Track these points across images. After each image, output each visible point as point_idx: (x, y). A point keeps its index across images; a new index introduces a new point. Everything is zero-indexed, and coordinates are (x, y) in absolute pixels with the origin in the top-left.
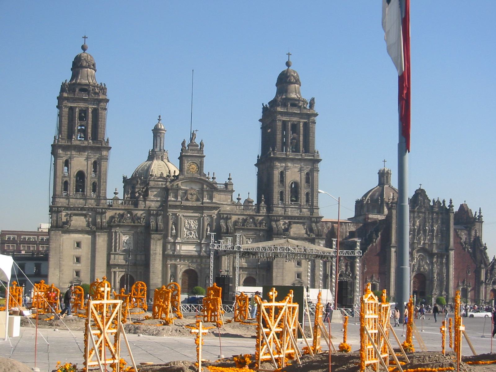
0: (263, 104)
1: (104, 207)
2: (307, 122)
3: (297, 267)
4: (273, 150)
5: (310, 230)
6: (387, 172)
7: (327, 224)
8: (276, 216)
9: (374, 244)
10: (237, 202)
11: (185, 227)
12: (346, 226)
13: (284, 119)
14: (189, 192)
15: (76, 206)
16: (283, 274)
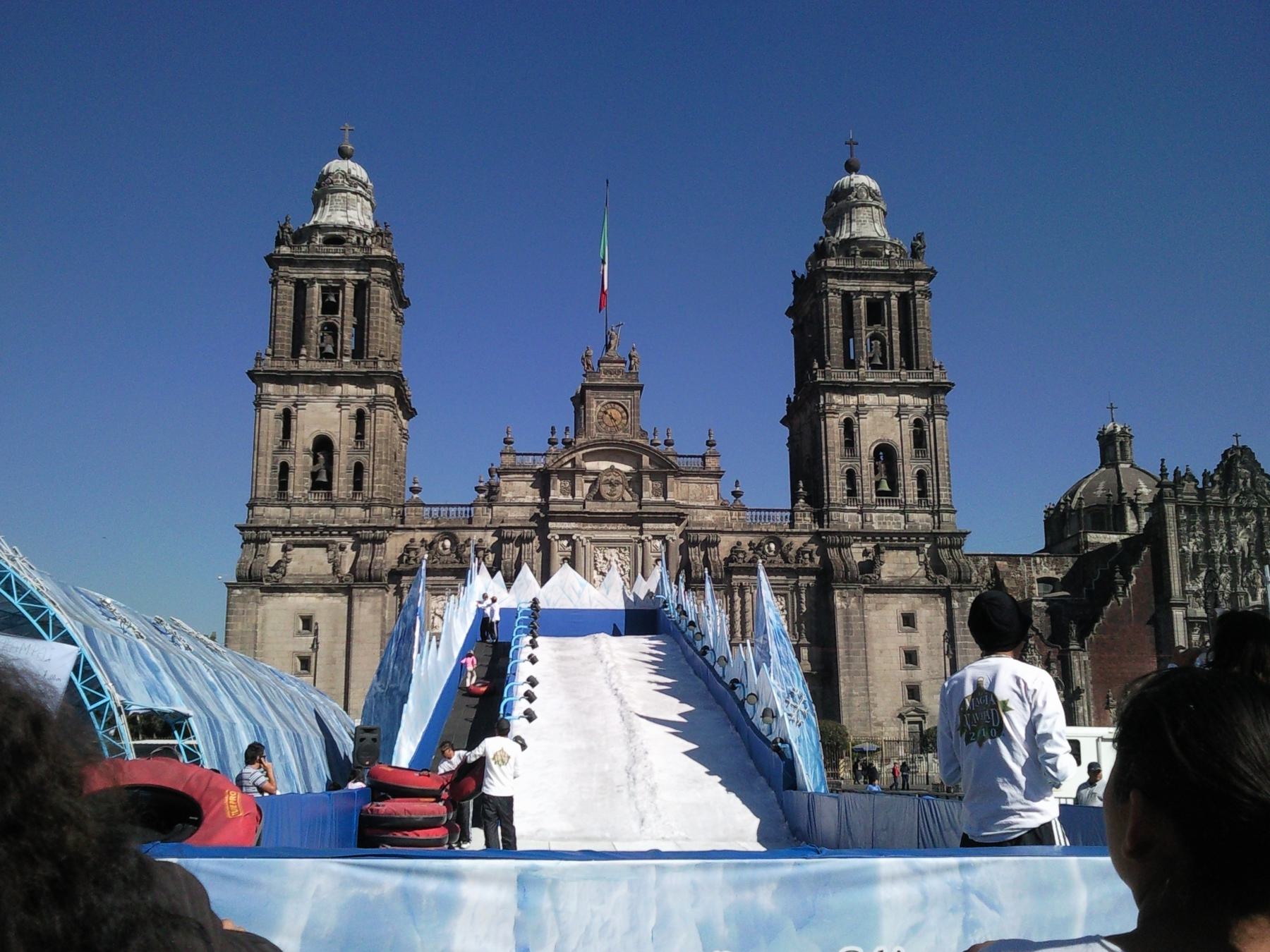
0: (794, 272)
1: (381, 525)
2: (907, 292)
3: (906, 669)
4: (822, 365)
5: (937, 567)
6: (1123, 431)
7: (978, 560)
8: (839, 534)
9: (1121, 599)
10: (732, 502)
11: (596, 569)
12: (1029, 564)
13: (846, 289)
14: (605, 478)
15: (310, 524)
16: (868, 690)
